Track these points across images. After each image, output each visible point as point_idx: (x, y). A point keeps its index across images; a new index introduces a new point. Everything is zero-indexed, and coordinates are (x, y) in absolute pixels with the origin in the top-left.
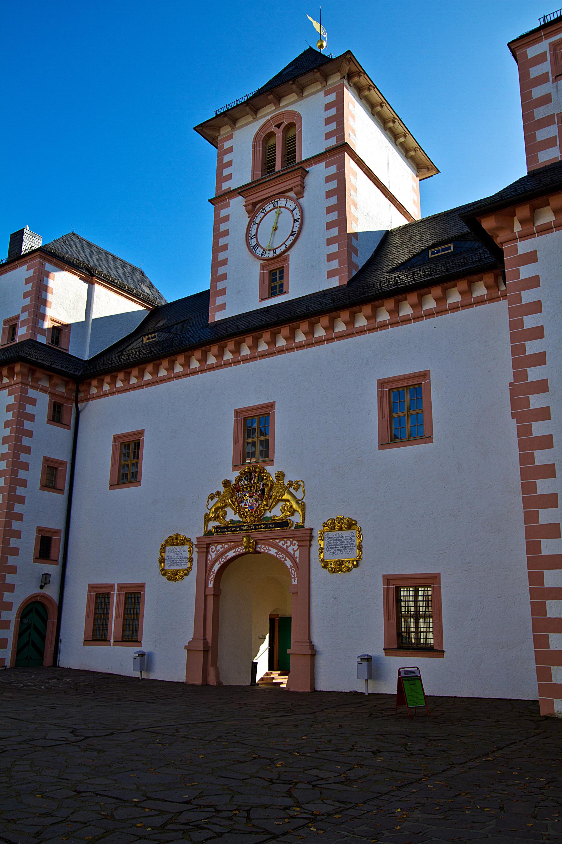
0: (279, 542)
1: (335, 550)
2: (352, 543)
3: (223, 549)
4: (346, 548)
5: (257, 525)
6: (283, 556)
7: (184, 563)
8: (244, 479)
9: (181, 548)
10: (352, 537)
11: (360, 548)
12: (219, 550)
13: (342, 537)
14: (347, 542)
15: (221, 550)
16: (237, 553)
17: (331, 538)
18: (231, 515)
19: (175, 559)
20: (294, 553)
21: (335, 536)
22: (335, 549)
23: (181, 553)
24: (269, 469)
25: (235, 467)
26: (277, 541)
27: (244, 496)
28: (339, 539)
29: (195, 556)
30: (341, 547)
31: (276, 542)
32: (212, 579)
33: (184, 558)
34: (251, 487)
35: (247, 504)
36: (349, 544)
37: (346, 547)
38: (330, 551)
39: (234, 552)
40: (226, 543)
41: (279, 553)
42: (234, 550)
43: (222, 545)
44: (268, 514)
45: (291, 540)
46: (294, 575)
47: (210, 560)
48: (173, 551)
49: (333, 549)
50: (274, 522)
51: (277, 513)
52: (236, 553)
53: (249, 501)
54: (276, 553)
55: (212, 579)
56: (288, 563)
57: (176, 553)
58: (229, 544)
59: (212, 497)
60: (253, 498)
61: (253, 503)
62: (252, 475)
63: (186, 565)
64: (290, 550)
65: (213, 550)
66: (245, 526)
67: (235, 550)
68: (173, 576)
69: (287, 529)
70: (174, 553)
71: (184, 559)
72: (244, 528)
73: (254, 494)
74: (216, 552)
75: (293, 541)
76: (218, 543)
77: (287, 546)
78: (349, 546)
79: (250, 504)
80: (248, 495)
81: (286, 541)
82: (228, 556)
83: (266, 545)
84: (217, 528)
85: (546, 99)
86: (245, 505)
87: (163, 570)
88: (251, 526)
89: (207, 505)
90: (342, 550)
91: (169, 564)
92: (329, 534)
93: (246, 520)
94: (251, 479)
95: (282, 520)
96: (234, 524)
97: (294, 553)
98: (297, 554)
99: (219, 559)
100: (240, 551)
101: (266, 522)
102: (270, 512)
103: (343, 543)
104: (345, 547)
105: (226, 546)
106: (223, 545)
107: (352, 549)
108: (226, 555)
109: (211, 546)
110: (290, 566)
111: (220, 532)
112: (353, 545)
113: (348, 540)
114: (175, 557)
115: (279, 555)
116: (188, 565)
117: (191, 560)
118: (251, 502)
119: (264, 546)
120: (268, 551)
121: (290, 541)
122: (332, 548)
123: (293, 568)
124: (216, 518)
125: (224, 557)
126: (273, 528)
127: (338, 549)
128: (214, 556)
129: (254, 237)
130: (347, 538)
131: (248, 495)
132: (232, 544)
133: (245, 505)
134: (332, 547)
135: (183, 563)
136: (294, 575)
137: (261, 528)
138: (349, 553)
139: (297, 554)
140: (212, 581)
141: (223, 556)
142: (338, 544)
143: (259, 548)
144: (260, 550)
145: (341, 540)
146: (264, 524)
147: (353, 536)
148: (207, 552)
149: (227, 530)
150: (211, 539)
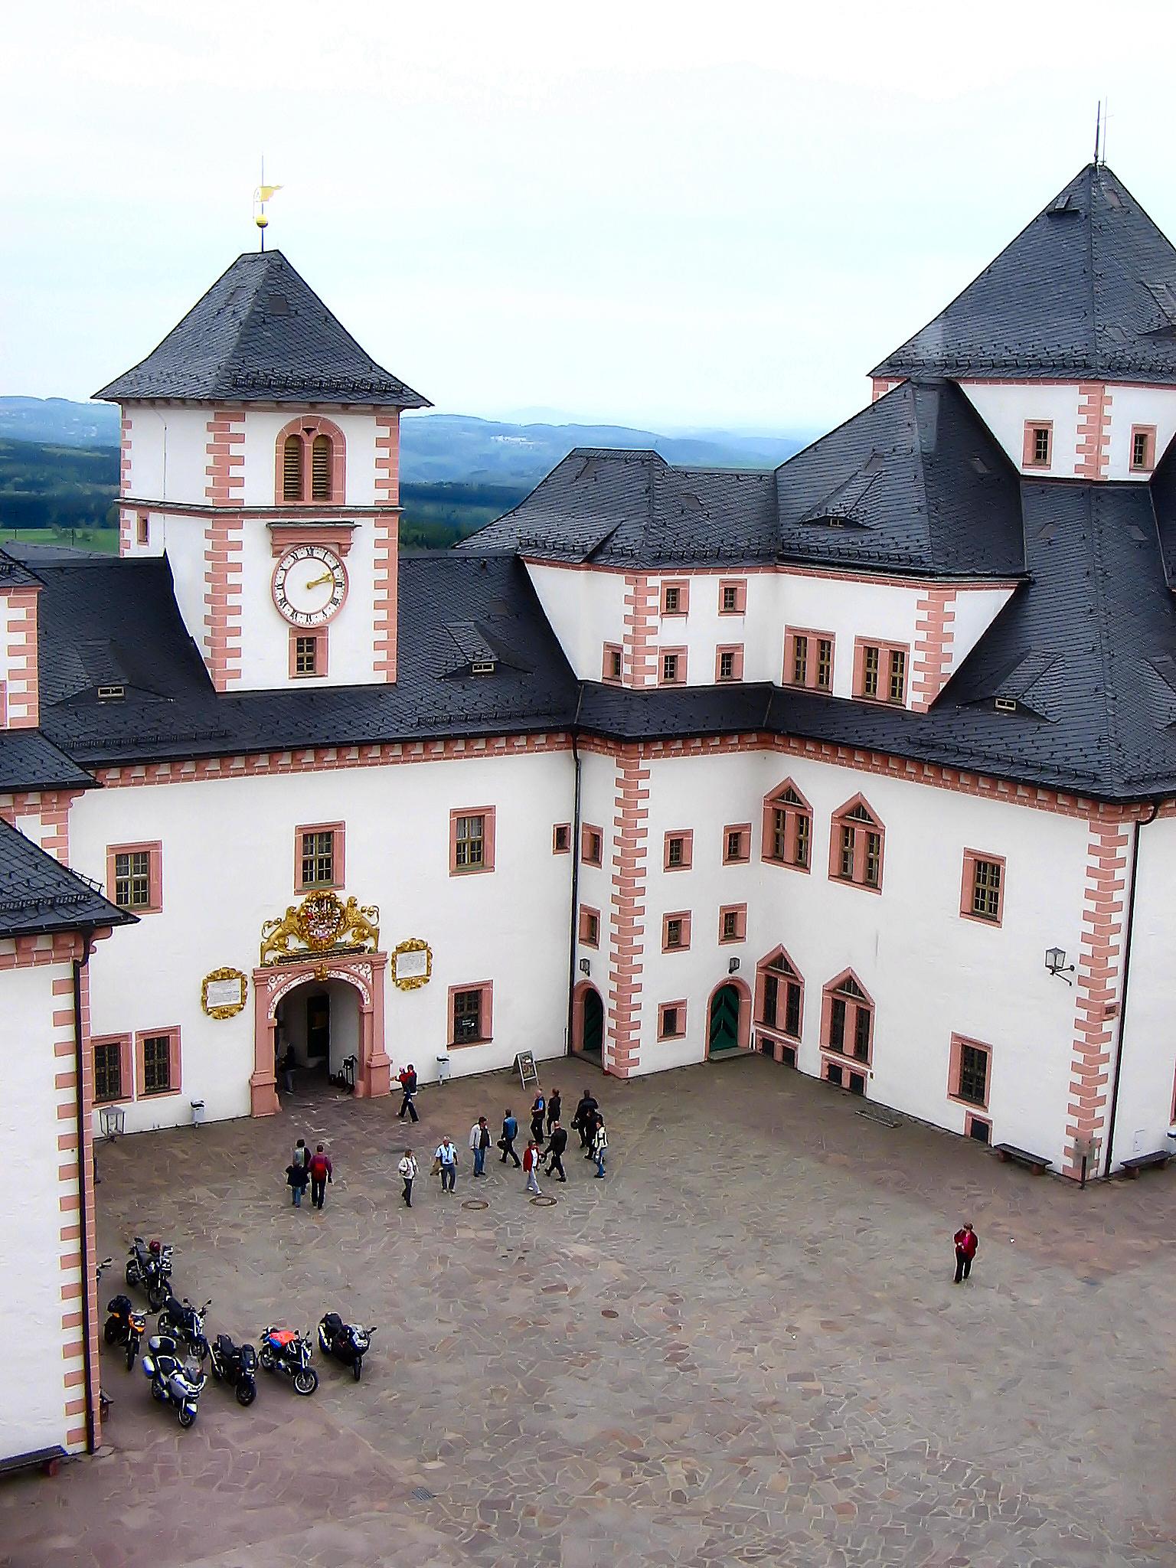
11: (429, 968)
15: (283, 980)
18: (295, 944)
24: (338, 893)
25: (298, 892)
29: (250, 989)
51: (348, 938)
56: (360, 986)
59: (269, 924)
64: (362, 973)
68: (224, 1013)
74: (276, 982)
84: (281, 959)
85: (654, 630)
105: (289, 975)
117: (244, 997)
128: (274, 986)
129: (281, 587)
139: (370, 976)
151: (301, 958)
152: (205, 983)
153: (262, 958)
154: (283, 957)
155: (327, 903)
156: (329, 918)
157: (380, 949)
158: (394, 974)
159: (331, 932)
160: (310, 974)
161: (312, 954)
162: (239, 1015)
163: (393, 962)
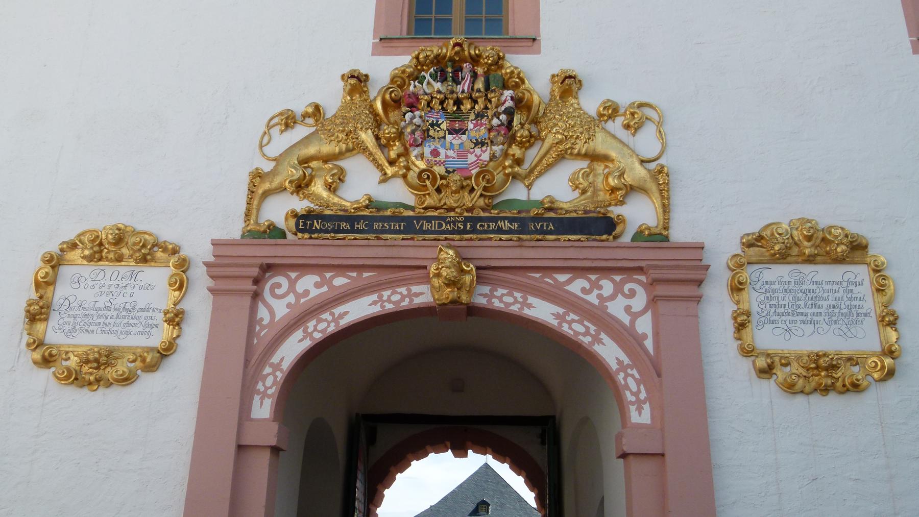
0: (569, 282)
1: (791, 322)
2: (854, 303)
3: (325, 289)
4: (834, 318)
5: (480, 219)
6: (587, 328)
7: (141, 329)
8: (431, 76)
9: (133, 276)
10: (851, 287)
11: (890, 320)
12: (307, 292)
13: (816, 283)
14: (836, 299)
15: (314, 293)
16: (389, 307)
17: (772, 283)
19: (100, 309)
20: (633, 322)
21: (787, 279)
22: (788, 318)
23: (129, 290)
24: (516, 61)
26: (562, 278)
27: (432, 125)
28: (804, 287)
30: (813, 314)
31: (555, 280)
32: (270, 392)
33: (143, 310)
34: (458, 102)
35: (442, 151)
36: (843, 306)
37: (831, 315)
38: (773, 322)
39: (374, 303)
40: (341, 268)
41: (568, 318)
42: (374, 297)
43: (323, 277)
44: (518, 192)
45: (618, 278)
46: (636, 394)
47: (265, 322)
48: (92, 283)
49: (783, 318)
50: (552, 215)
52: (382, 306)
53: (448, 145)
54: (557, 316)
55: (270, 392)
57: (105, 289)
58: (354, 274)
60: (464, 137)
61: (462, 154)
62: (461, 69)
63: (149, 334)
64: (617, 309)
65: (278, 292)
66: (429, 219)
67: (380, 297)
69: (607, 240)
70: (97, 289)
71: (139, 314)
72: (426, 226)
73: (471, 126)
74: (291, 298)
75: (623, 282)
76: (304, 268)
77: (600, 296)
78: (845, 311)
79: (451, 153)
80: (444, 126)
81: (598, 280)
82: (346, 313)
83: (513, 286)
86: (435, 153)
87: (38, 344)
88: (454, 223)
89: (261, 147)
90: (818, 322)
91: (67, 328)
92: (765, 272)
93: (440, 200)
94: (456, 81)
95: (586, 212)
96: (379, 210)
97: (633, 322)
98: (644, 325)
99: (309, 320)
100: (402, 299)
101: (519, 212)
102: (529, 187)
103: (820, 303)
104: (831, 315)
105: (340, 281)
106: (328, 275)
107: (857, 322)
108: (338, 311)
109: (271, 277)
110: (620, 362)
111: (320, 231)
112: (860, 311)
113: (836, 295)
114: (97, 305)
115: (570, 323)
116: (161, 335)
118: (457, 147)
119: (505, 291)
120: (521, 309)
121: (613, 281)
122: (780, 315)
123: (629, 371)
124: (301, 186)
125: (326, 316)
126: (551, 233)
127: (804, 318)
130: (836, 287)
131: (444, 126)
132: (365, 275)
133: (435, 153)
134: (779, 310)
135: (134, 325)
136: (636, 394)
137: (500, 231)
138: (849, 334)
140: (269, 396)
141: (324, 311)
142: (802, 303)
143: (485, 295)
144: (489, 301)
145: (814, 291)
146: (512, 220)
147: (856, 284)
148: (256, 296)
149: (352, 226)
150: (280, 251)
151: (376, 226)
152: (55, 262)
153: (248, 214)
154: (321, 217)
155: (475, 76)
156: (479, 116)
157: (679, 233)
158: (741, 327)
159: (486, 157)
160: (415, 289)
161: (419, 218)
162: (149, 383)
163: (737, 288)
